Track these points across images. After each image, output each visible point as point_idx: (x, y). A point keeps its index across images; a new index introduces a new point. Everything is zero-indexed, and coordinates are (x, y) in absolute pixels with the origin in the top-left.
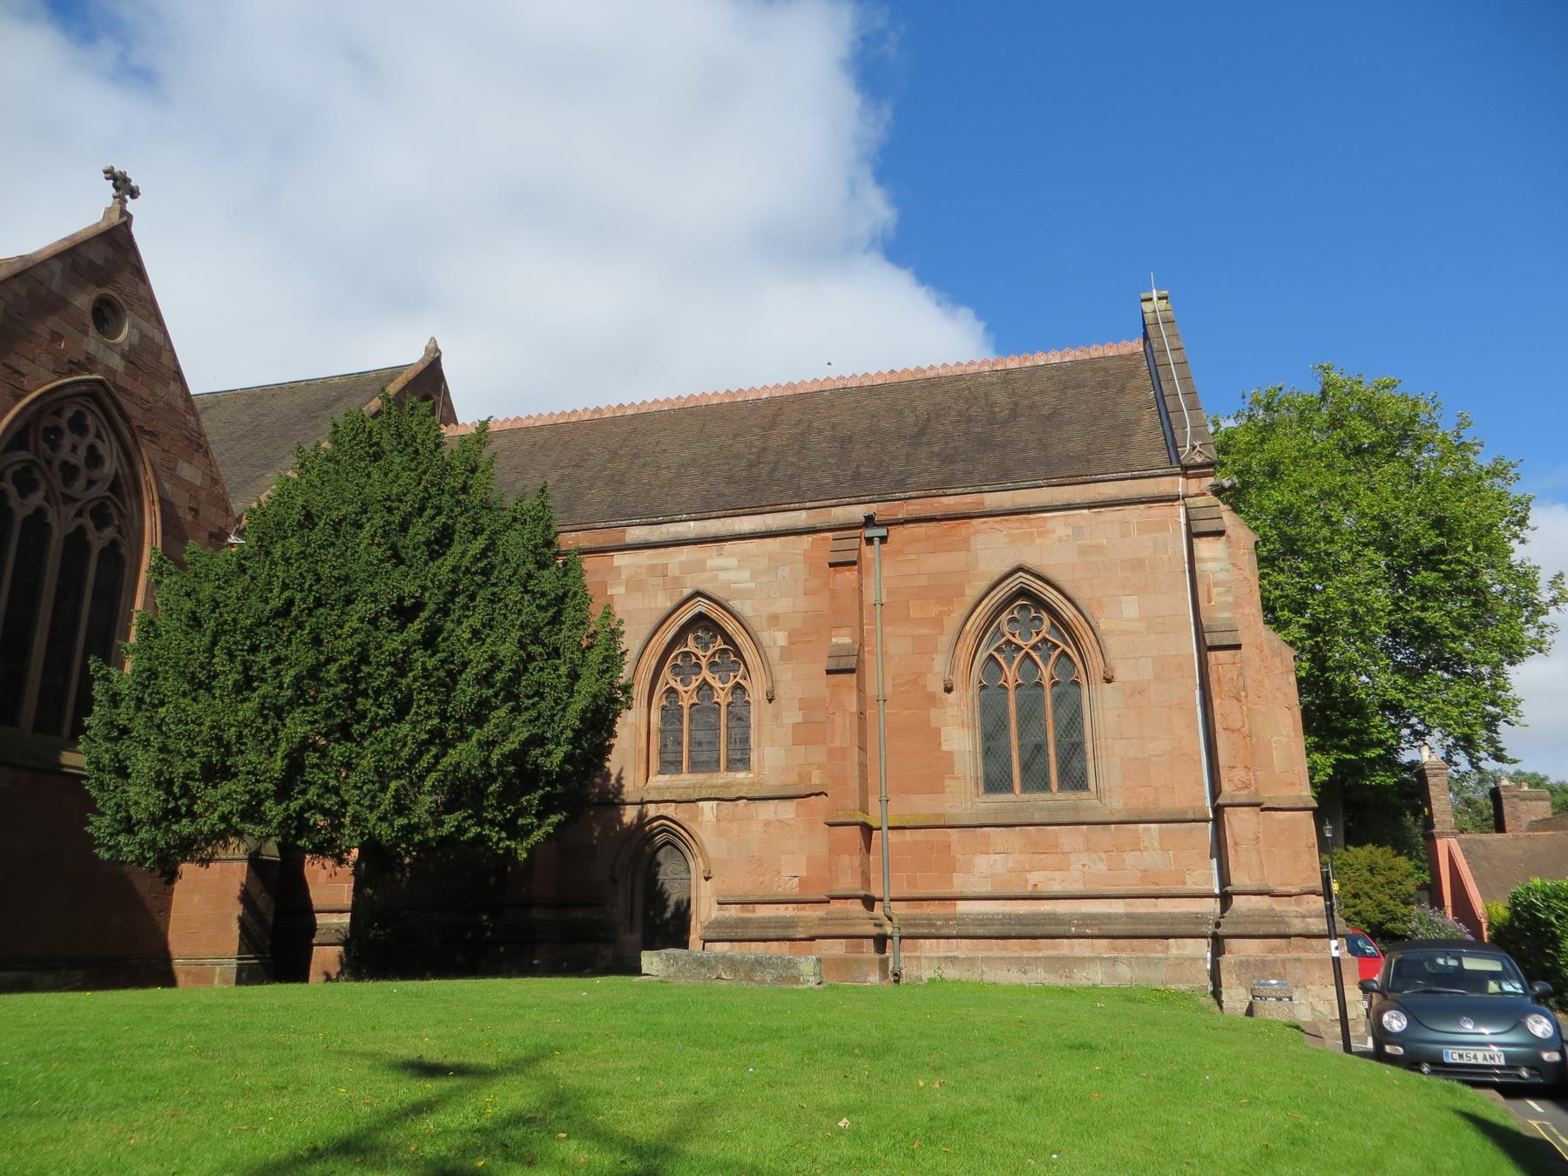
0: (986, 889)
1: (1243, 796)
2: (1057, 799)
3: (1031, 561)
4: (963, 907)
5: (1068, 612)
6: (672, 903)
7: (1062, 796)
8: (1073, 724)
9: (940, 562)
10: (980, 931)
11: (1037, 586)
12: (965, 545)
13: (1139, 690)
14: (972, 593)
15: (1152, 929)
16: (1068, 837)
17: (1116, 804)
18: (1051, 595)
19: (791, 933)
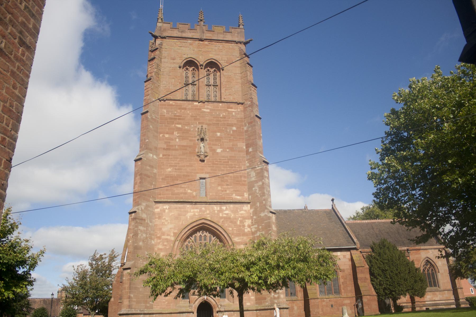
0: (429, 300)
1: (459, 287)
2: (434, 288)
3: (428, 256)
4: (426, 303)
5: (433, 263)
6: (387, 304)
7: (430, 288)
8: (434, 278)
9: (417, 256)
10: (430, 305)
11: (429, 260)
12: (420, 254)
13: (442, 274)
14: (421, 260)
15: (449, 304)
16: (437, 293)
17: (442, 288)
18: (431, 261)
19: (407, 307)
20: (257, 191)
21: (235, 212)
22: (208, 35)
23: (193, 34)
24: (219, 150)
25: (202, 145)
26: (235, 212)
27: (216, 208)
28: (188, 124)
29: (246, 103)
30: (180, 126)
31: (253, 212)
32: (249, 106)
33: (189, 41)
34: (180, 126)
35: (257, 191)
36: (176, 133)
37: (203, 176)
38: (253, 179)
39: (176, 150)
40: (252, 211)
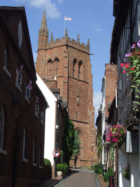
20: (92, 120)
21: (85, 126)
22: (80, 48)
23: (76, 46)
24: (82, 101)
25: (78, 98)
26: (85, 126)
27: (80, 124)
28: (74, 89)
29: (90, 83)
30: (72, 89)
31: (89, 127)
32: (91, 85)
33: (75, 50)
34: (72, 89)
35: (92, 120)
36: (71, 92)
37: (77, 111)
38: (90, 115)
39: (71, 99)
40: (89, 126)
